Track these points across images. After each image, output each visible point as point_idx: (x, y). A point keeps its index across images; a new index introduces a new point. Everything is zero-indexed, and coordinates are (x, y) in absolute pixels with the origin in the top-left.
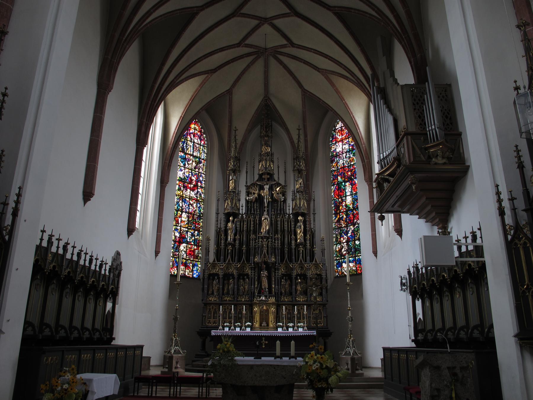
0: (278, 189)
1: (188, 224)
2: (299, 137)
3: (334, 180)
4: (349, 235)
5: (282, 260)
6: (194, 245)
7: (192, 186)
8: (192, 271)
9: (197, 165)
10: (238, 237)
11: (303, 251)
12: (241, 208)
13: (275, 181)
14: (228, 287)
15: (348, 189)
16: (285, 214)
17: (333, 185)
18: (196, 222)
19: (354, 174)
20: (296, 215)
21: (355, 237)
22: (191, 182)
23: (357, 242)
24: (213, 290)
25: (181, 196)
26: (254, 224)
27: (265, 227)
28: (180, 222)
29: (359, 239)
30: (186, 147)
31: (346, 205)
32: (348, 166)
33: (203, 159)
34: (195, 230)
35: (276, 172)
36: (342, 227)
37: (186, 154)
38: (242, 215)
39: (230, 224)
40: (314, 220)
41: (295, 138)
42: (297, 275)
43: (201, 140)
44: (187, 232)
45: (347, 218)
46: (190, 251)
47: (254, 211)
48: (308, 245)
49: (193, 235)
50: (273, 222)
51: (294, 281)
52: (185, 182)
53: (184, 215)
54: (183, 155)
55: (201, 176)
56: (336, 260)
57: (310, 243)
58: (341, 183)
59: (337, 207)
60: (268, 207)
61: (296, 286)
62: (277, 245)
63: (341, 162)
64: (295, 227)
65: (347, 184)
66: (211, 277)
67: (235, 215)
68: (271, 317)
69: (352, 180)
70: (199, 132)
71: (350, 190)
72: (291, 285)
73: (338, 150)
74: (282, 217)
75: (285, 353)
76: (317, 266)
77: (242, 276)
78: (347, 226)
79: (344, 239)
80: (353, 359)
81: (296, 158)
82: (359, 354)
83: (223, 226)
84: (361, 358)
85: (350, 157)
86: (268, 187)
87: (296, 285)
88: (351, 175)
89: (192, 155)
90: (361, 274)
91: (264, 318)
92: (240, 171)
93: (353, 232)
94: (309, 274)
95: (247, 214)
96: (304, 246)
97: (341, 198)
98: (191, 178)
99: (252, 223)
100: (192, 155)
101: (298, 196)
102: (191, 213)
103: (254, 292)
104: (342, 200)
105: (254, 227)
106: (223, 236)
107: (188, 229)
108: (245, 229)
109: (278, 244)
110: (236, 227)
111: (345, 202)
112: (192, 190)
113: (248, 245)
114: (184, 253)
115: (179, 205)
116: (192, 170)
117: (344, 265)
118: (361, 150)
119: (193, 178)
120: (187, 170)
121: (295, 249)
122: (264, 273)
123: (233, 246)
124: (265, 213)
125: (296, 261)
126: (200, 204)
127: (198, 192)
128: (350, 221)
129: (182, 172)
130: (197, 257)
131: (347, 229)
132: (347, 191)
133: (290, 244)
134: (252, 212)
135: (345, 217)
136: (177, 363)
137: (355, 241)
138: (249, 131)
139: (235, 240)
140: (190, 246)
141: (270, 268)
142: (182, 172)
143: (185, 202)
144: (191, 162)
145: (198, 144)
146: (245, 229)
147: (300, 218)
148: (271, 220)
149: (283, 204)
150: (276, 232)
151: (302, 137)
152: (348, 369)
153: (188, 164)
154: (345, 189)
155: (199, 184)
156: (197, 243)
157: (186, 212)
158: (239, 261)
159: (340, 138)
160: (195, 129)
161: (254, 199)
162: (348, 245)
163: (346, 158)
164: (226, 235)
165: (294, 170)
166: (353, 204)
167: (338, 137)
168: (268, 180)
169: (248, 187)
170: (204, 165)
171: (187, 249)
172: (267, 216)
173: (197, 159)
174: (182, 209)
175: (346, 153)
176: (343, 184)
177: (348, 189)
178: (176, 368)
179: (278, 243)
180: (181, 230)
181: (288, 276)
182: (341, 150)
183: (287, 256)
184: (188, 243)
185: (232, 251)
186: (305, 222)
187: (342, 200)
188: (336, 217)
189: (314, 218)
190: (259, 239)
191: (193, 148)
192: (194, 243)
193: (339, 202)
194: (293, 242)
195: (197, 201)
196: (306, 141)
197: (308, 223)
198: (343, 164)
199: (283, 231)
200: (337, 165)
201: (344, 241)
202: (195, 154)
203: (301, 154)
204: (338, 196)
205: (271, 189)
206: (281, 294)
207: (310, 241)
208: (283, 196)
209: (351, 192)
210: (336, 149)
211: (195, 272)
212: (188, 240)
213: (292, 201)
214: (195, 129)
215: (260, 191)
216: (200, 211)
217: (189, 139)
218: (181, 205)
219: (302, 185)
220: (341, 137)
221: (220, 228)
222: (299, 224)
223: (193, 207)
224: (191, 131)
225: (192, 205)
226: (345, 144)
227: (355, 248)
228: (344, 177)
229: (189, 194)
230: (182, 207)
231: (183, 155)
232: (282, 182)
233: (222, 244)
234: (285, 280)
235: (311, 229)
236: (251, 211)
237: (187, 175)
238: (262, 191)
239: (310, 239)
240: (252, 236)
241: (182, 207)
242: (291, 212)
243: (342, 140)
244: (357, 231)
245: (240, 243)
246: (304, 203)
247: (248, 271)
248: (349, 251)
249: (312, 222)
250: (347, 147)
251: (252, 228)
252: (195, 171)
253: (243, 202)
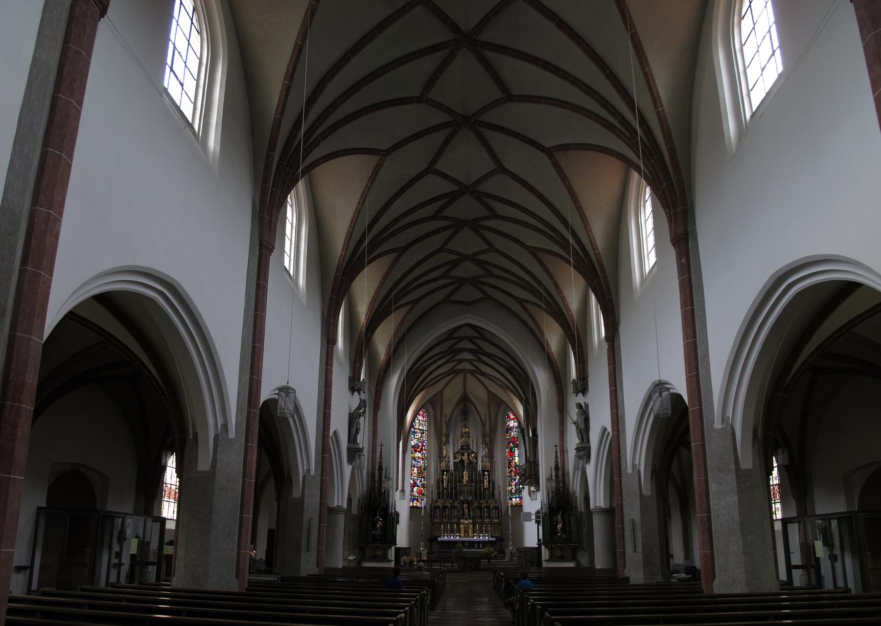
16: (477, 471)
20: (484, 471)
27: (466, 478)
41: (483, 418)
52: (415, 448)
67: (448, 471)
68: (470, 531)
75: (479, 548)
76: (496, 502)
77: (453, 507)
81: (484, 436)
91: (466, 531)
94: (491, 506)
109: (473, 489)
113: (456, 489)
123: (447, 489)
130: (423, 495)
133: (480, 489)
141: (469, 503)
150: (472, 482)
156: (423, 486)
169: (455, 454)
196: (490, 420)
199: (476, 481)
205: (468, 455)
232: (475, 450)
240: (458, 484)
247: (456, 504)
248: (516, 490)
253: (452, 463)
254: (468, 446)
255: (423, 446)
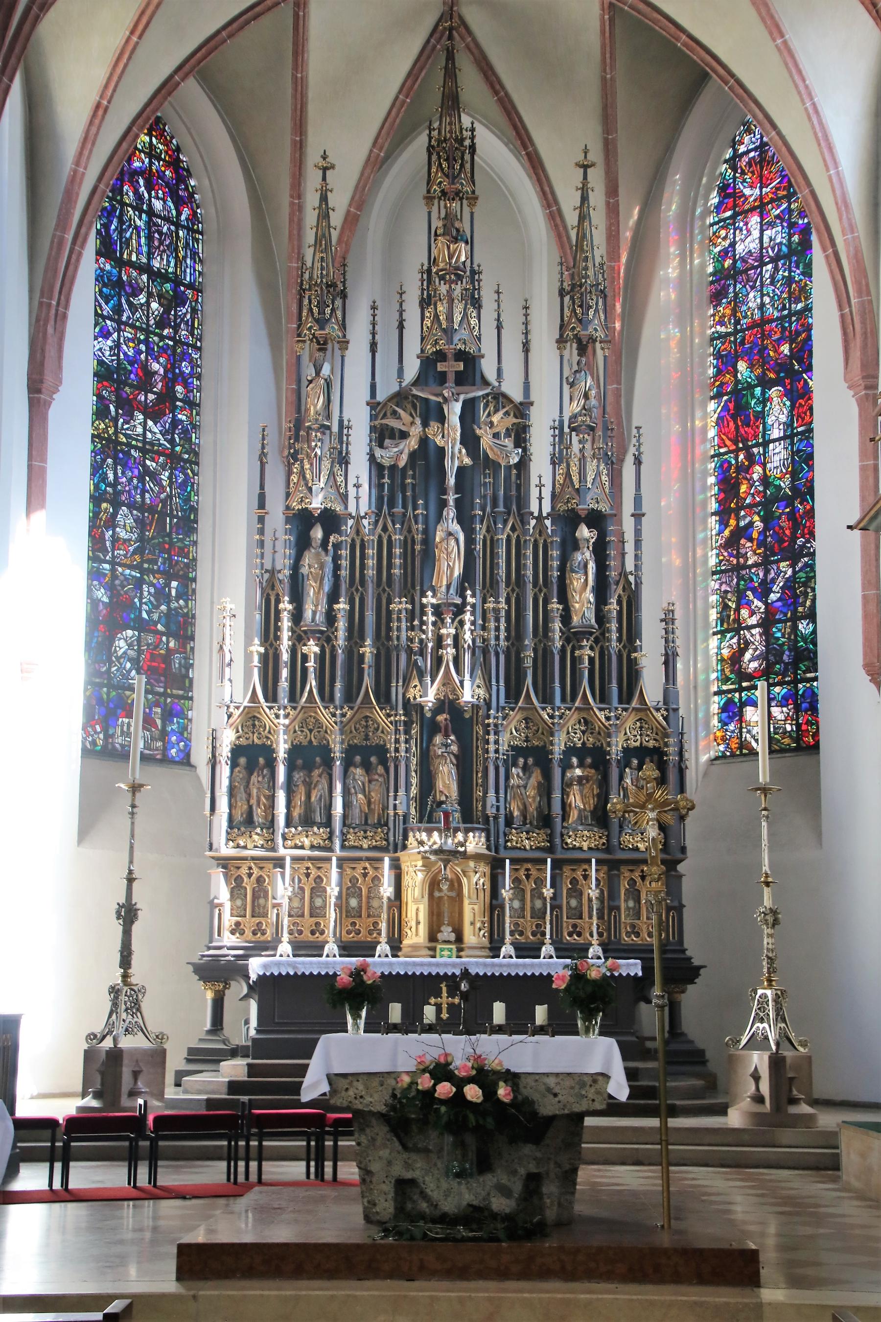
0: (495, 419)
1: (139, 551)
2: (584, 199)
3: (719, 373)
4: (773, 597)
5: (514, 692)
6: (168, 634)
7: (151, 397)
8: (164, 735)
9: (167, 311)
10: (342, 606)
11: (591, 660)
12: (352, 492)
13: (486, 383)
14: (308, 796)
15: (778, 413)
16: (523, 516)
17: (718, 396)
18: (171, 544)
19: (803, 353)
20: (569, 520)
21: (795, 604)
22: (145, 385)
23: (804, 627)
24: (250, 807)
25: (108, 440)
26: (404, 556)
28: (108, 544)
29: (812, 616)
30: (121, 232)
31: (765, 480)
32: (781, 318)
33: (191, 286)
34: (169, 578)
35: (488, 347)
36: (745, 567)
37: (121, 263)
38: (359, 519)
39: (308, 559)
40: (638, 543)
42: (570, 751)
43: (179, 203)
44: (139, 584)
45: (766, 528)
46: (153, 657)
47: (405, 506)
48: (614, 636)
49: (162, 595)
50: (479, 547)
51: (557, 772)
53: (126, 518)
54: (108, 267)
55: (185, 356)
56: (719, 693)
57: (619, 630)
58: (750, 387)
59: (728, 485)
60: (459, 488)
61: (564, 793)
62: (493, 633)
63: (753, 299)
64: (562, 569)
65: (774, 392)
66: (243, 761)
69: (795, 376)
70: (168, 165)
71: (783, 418)
72: (545, 790)
73: (740, 249)
74: (513, 529)
78: (765, 563)
79: (752, 613)
80: (777, 1063)
82: (804, 1044)
83: (283, 564)
84: (809, 1059)
85: (790, 280)
86: (457, 407)
87: (566, 786)
88: (791, 357)
89: (146, 269)
90: (815, 748)
92: (344, 344)
93: (790, 585)
94: (616, 749)
95: (378, 515)
96: (597, 641)
97: (747, 449)
98: (145, 367)
99: (397, 551)
100: (146, 269)
101: (576, 447)
102: (152, 509)
103: (406, 817)
104: (750, 457)
105: (404, 566)
106: (286, 605)
107: (143, 572)
108: (371, 572)
110: (337, 568)
111: (764, 465)
112: (153, 413)
113: (383, 634)
114: (128, 665)
115: (104, 478)
116: (147, 332)
117: (750, 714)
118: (836, 254)
119: (155, 366)
120: (128, 333)
121: (563, 650)
122: (444, 746)
123: (326, 639)
124: (450, 512)
125: (563, 700)
126: (183, 470)
127: (175, 423)
128: (781, 541)
129: (109, 343)
131: (767, 572)
132: (770, 420)
133: (543, 632)
134: (399, 510)
135: (759, 525)
136: (136, 1075)
137: (795, 619)
138: (378, 162)
139: (331, 618)
140: (150, 639)
142: (109, 343)
143: (125, 467)
144: (142, 298)
145: (167, 219)
146: (371, 572)
147: (584, 532)
148: (470, 541)
149: (518, 476)
151: (597, 198)
152: (758, 1099)
153: (133, 308)
154: (761, 416)
155: (179, 388)
157: (131, 506)
158: (349, 697)
159: (751, 193)
160: (151, 152)
161: (404, 458)
162: (767, 634)
163: (772, 283)
164: (297, 598)
165: (561, 341)
166: (794, 475)
167: (747, 192)
168: (461, 379)
170: (194, 311)
171: (139, 652)
172: (456, 527)
173: (168, 286)
174: (117, 494)
175: (774, 260)
176: (758, 391)
177: (778, 413)
178: (133, 1094)
179: (497, 629)
180: (114, 577)
181: (534, 755)
182: (754, 246)
183: (529, 680)
184: (142, 626)
185: (321, 658)
186: (600, 550)
187: (750, 457)
188: (724, 523)
189: (638, 532)
190: (423, 613)
191: (150, 238)
192: (166, 626)
193: (740, 468)
194: (557, 625)
195: (173, 460)
197: (612, 553)
198: (762, 306)
200: (734, 312)
201: (753, 621)
202: (156, 264)
203: (590, 273)
204: (735, 443)
206: (509, 821)
207: (620, 621)
208: (517, 446)
209: (789, 425)
210: (733, 245)
211: (174, 738)
212: (145, 615)
213: (553, 463)
214: (151, 152)
215: (425, 424)
216: (188, 500)
217: (129, 197)
218: (111, 476)
219: (593, 402)
220: (757, 191)
221: (272, 572)
222: (578, 557)
223: (159, 483)
224: (137, 164)
225: (154, 476)
226: (771, 225)
227: (794, 648)
228: (764, 360)
229: (140, 430)
230: (114, 485)
231: (108, 267)
232: (513, 389)
233: (285, 635)
234: (525, 768)
235: (623, 574)
236: (392, 504)
237: (131, 353)
238: (434, 426)
239: (620, 613)
240: (400, 605)
241: (114, 485)
242: (547, 508)
243: (761, 207)
244: (805, 584)
245: (350, 629)
246: (598, 474)
248: (771, 654)
249: (629, 547)
250: (777, 234)
251: (396, 571)
252: (162, 338)
253: (359, 469)
254: (469, 368)
255: (173, 377)
